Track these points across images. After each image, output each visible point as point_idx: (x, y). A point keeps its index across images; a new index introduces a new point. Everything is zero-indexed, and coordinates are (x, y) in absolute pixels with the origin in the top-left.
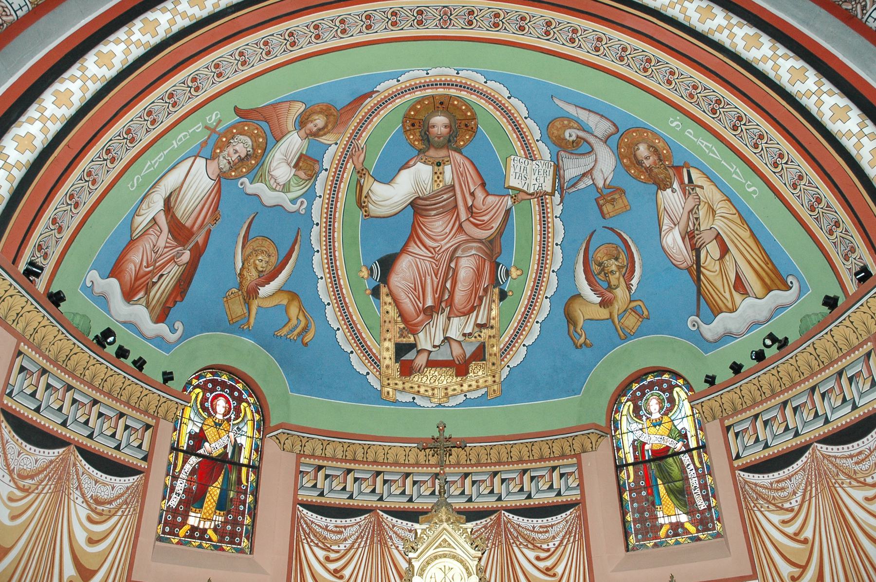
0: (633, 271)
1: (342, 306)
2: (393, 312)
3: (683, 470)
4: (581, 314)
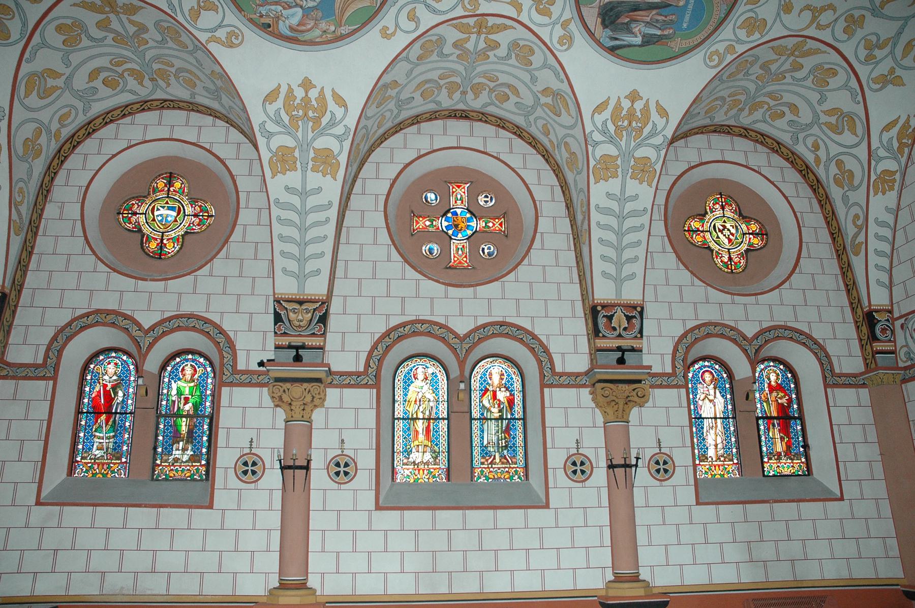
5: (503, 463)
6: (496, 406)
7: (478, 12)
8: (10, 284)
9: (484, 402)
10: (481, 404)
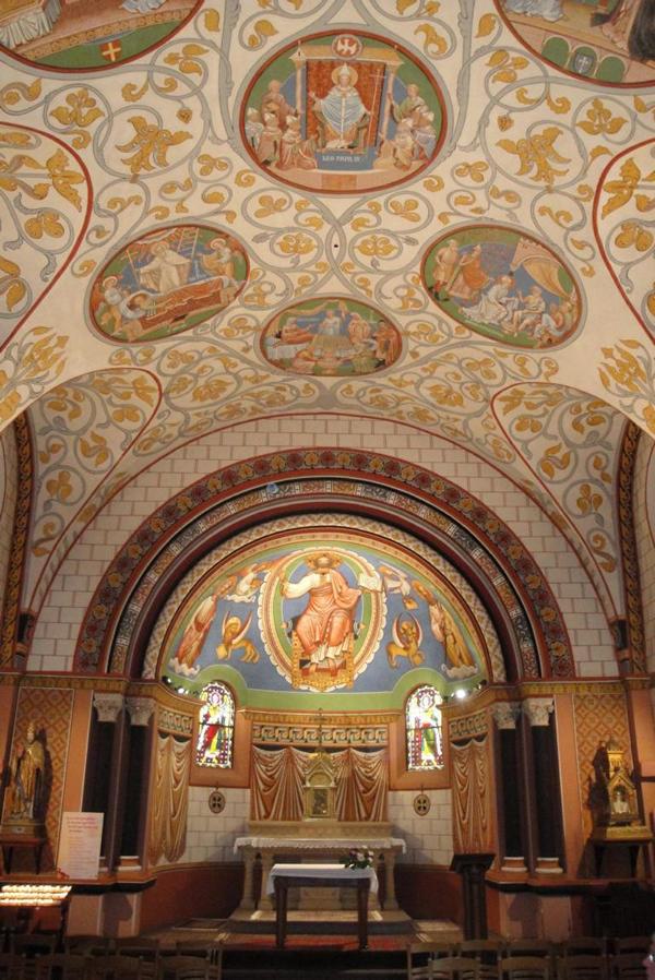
0: (418, 637)
1: (273, 643)
2: (298, 643)
3: (435, 735)
4: (395, 652)
7: (595, 189)
8: (624, 611)
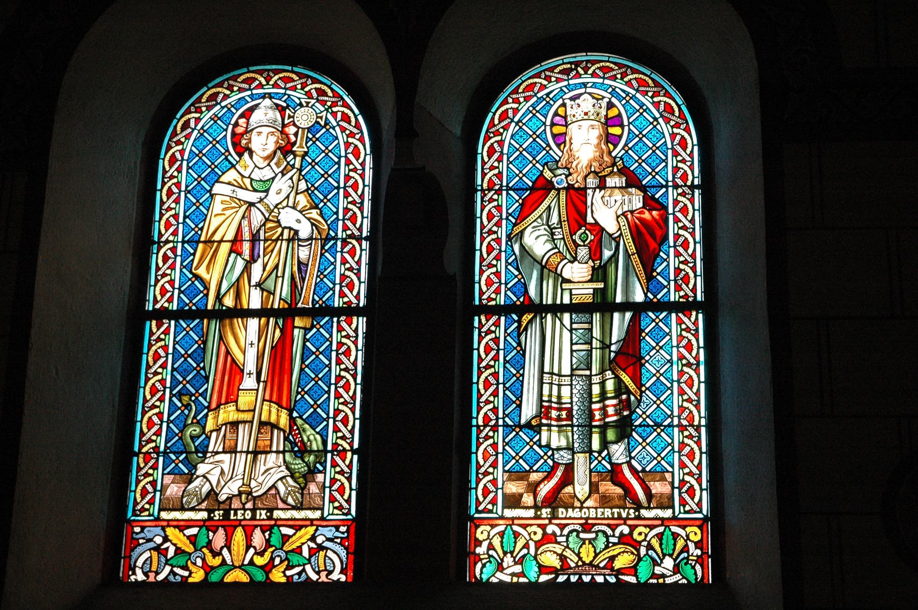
5: (605, 501)
6: (583, 252)
9: (529, 239)
10: (516, 247)
